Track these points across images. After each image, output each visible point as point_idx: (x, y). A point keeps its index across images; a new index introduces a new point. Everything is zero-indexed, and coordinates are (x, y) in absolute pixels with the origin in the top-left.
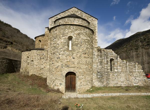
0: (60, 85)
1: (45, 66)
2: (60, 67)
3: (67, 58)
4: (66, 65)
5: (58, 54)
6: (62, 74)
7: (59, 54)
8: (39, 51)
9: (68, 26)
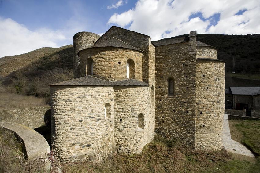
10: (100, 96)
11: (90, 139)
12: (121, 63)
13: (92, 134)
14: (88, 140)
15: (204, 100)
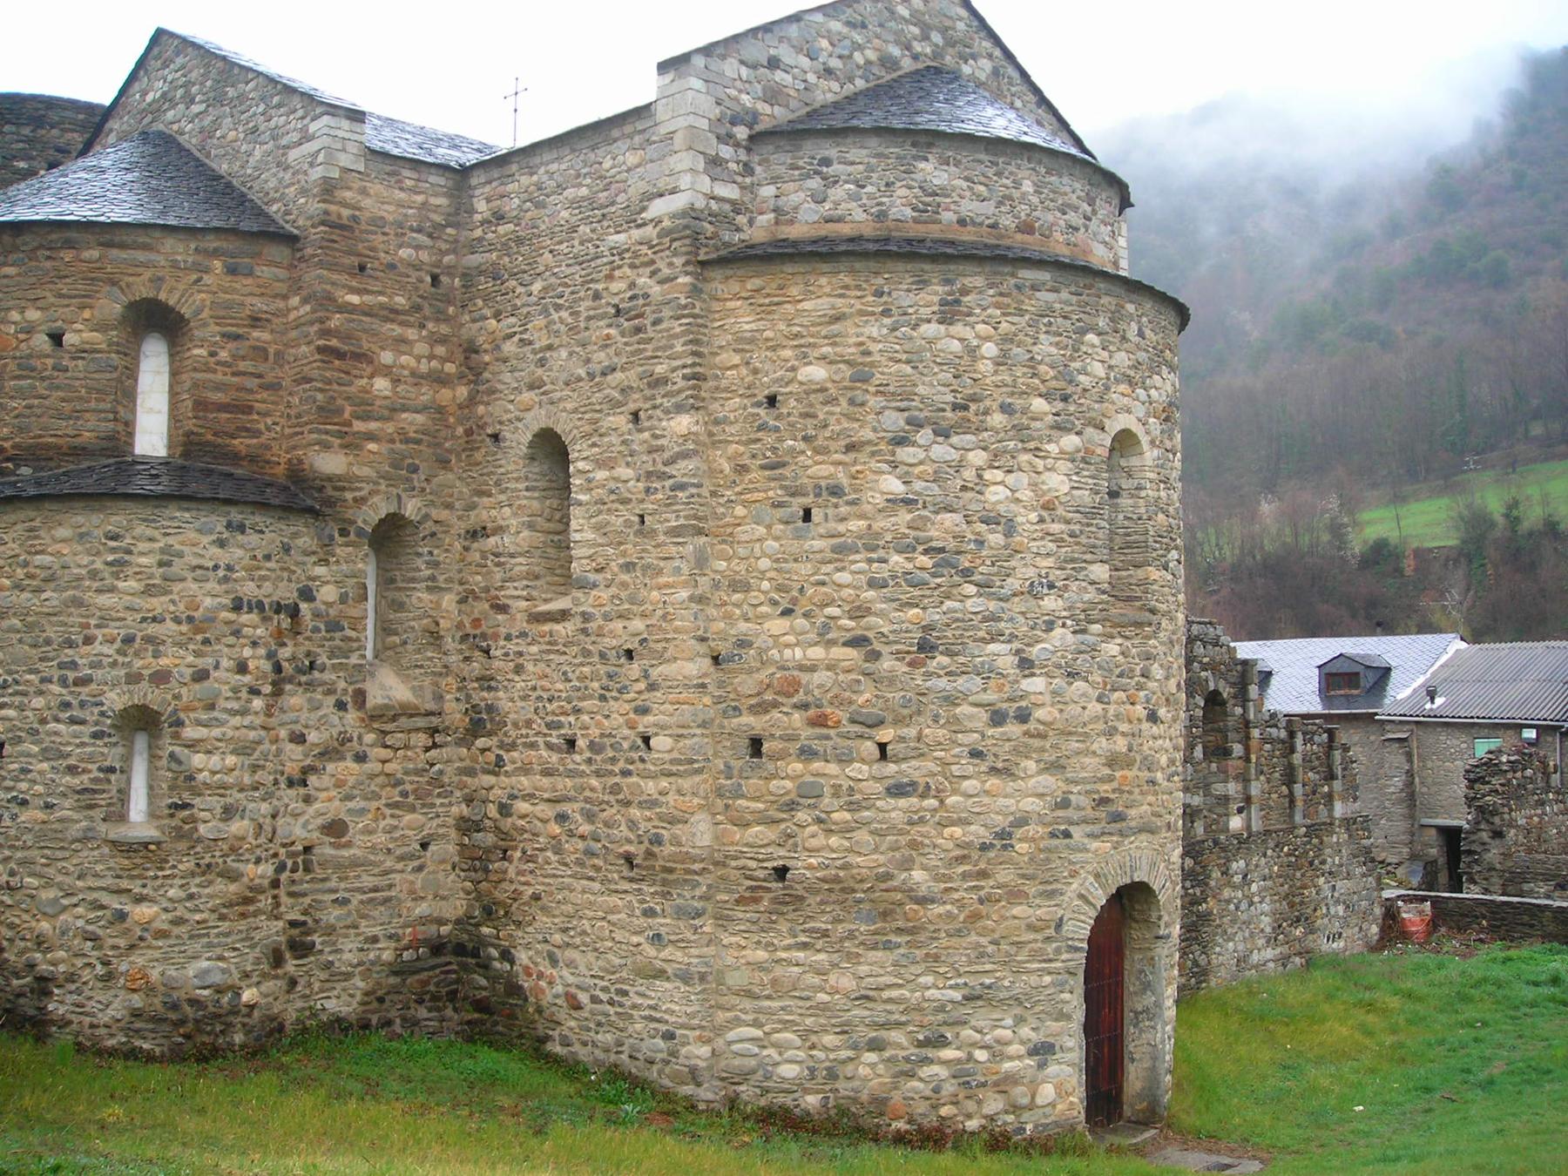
0: (1042, 1066)
2: (1033, 829)
3: (1112, 709)
4: (1104, 801)
5: (1007, 663)
6: (1059, 924)
7: (1026, 665)
8: (252, 539)
9: (1105, 300)
12: (69, 338)
15: (778, 625)
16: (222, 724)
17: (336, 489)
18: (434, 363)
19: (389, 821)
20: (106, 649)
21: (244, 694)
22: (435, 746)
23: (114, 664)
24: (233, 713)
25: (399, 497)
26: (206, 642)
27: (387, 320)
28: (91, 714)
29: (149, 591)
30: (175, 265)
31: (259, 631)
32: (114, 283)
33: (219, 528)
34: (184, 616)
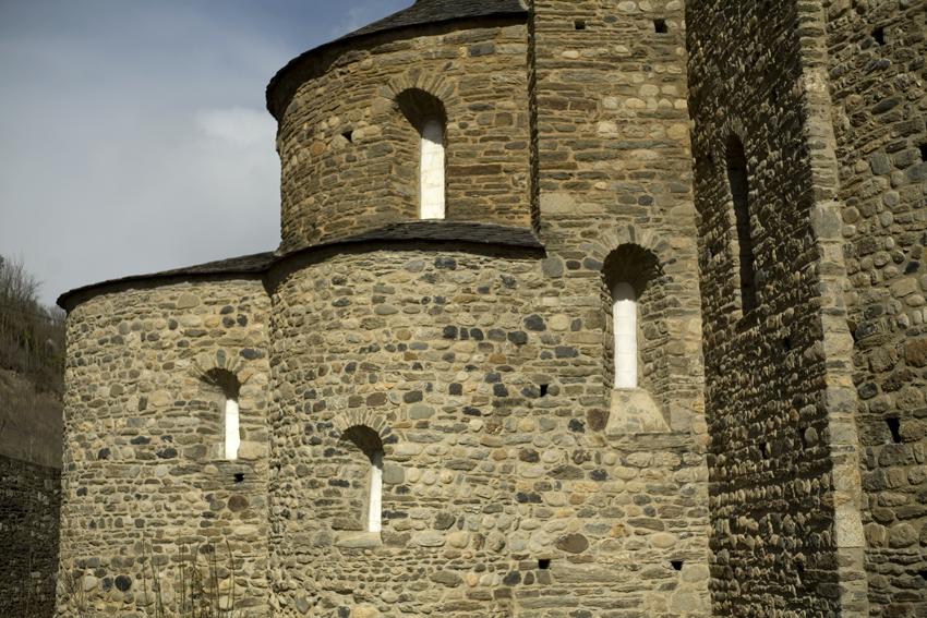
1: (574, 524)
10: (180, 329)
11: (131, 553)
12: (357, 134)
13: (140, 524)
14: (122, 552)
16: (438, 440)
17: (562, 226)
18: (664, 102)
19: (634, 538)
20: (336, 378)
21: (460, 415)
22: (683, 465)
23: (340, 391)
24: (448, 430)
25: (631, 229)
26: (417, 366)
27: (606, 68)
28: (324, 436)
29: (365, 325)
30: (428, 57)
31: (475, 357)
32: (385, 83)
33: (428, 265)
34: (396, 345)
